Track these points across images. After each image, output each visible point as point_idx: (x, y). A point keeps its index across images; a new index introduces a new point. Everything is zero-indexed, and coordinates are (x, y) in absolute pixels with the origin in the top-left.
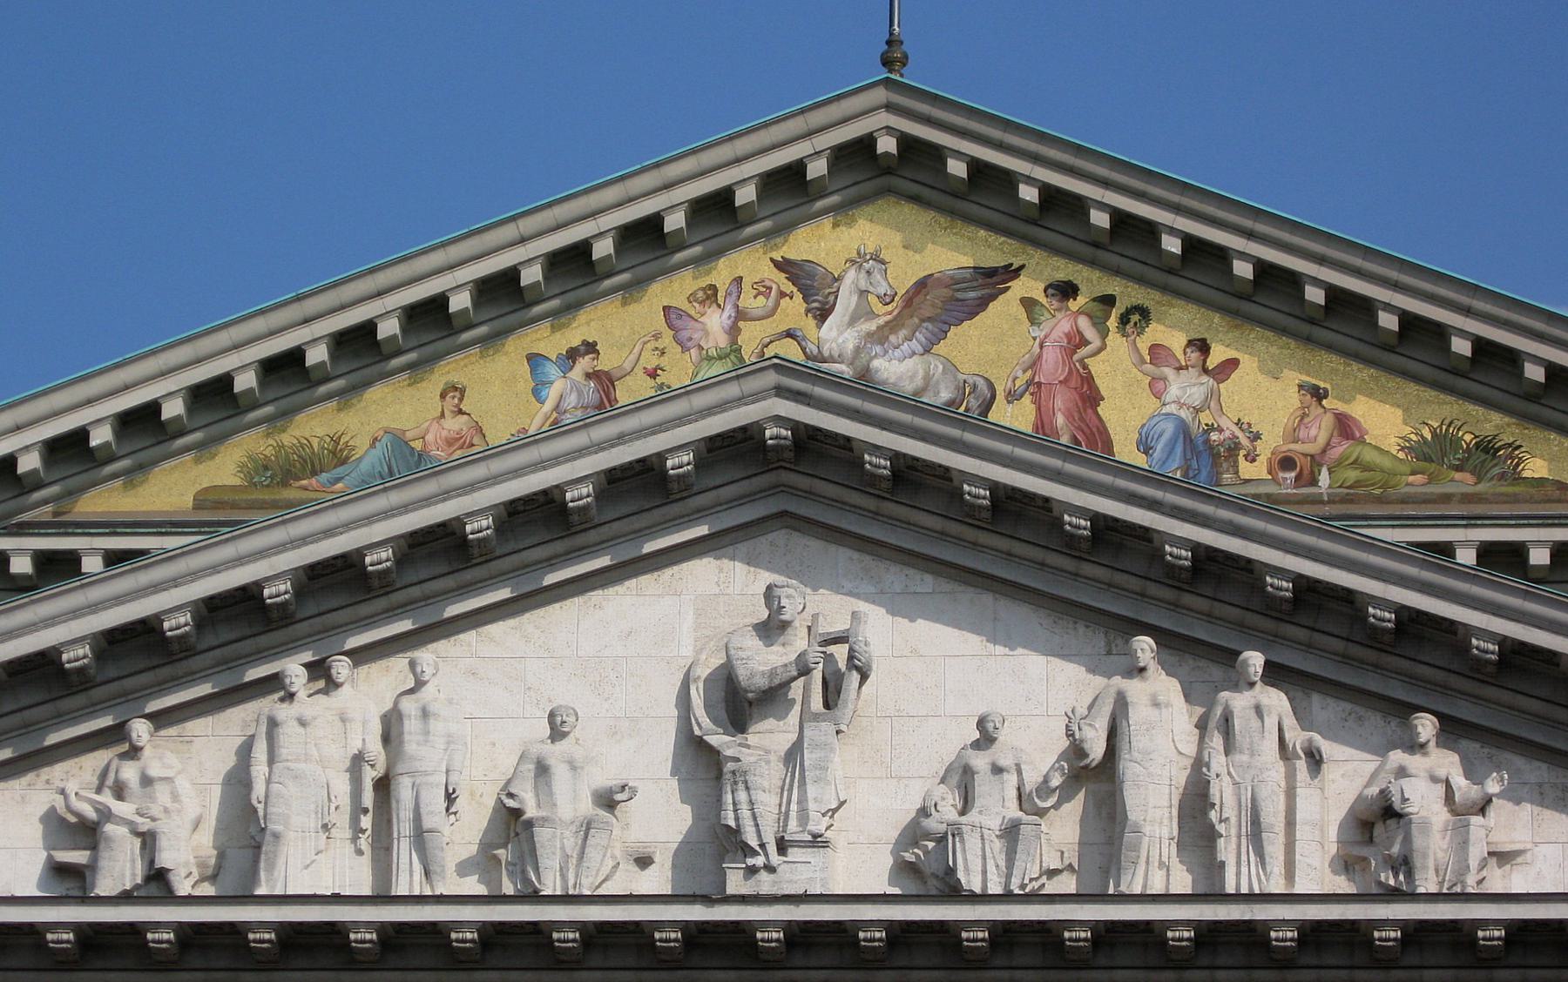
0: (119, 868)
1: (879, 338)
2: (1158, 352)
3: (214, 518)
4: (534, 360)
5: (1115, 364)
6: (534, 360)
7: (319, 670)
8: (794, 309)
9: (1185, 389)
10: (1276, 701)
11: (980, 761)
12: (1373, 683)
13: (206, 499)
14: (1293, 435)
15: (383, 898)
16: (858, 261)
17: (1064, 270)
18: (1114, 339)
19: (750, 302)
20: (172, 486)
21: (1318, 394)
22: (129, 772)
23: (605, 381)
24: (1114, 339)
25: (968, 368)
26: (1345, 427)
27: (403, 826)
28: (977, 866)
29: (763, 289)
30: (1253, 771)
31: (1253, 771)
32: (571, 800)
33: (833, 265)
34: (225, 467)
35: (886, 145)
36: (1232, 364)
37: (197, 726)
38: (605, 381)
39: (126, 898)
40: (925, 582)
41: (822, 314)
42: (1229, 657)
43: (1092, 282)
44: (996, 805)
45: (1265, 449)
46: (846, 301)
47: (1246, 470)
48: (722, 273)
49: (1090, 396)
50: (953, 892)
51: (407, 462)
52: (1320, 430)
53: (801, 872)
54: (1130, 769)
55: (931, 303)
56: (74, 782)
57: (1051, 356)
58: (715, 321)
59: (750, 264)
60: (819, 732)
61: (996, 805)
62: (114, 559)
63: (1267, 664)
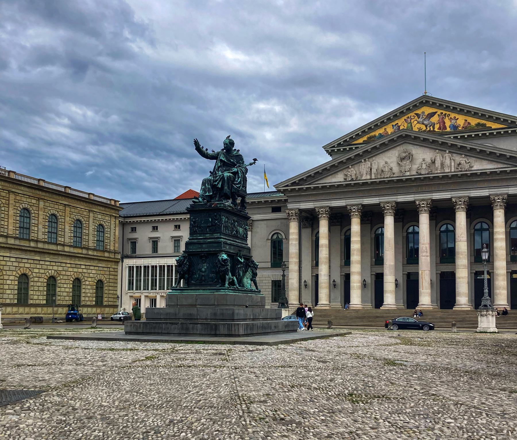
1: (424, 120)
3: (365, 142)
7: (365, 160)
9: (453, 121)
11: (423, 162)
12: (459, 152)
14: (464, 125)
15: (371, 179)
18: (447, 118)
19: (412, 117)
20: (361, 141)
21: (466, 120)
22: (350, 170)
24: (447, 118)
25: (433, 122)
26: (469, 123)
27: (373, 172)
28: (423, 172)
29: (413, 116)
30: (448, 162)
32: (387, 169)
34: (365, 138)
37: (355, 166)
38: (399, 126)
39: (350, 181)
42: (445, 151)
43: (444, 112)
45: (461, 126)
46: (421, 117)
48: (409, 115)
50: (421, 174)
51: (381, 136)
52: (467, 124)
53: (408, 174)
56: (345, 172)
58: (409, 120)
59: (412, 114)
60: (408, 161)
61: (424, 166)
62: (356, 148)
63: (449, 152)
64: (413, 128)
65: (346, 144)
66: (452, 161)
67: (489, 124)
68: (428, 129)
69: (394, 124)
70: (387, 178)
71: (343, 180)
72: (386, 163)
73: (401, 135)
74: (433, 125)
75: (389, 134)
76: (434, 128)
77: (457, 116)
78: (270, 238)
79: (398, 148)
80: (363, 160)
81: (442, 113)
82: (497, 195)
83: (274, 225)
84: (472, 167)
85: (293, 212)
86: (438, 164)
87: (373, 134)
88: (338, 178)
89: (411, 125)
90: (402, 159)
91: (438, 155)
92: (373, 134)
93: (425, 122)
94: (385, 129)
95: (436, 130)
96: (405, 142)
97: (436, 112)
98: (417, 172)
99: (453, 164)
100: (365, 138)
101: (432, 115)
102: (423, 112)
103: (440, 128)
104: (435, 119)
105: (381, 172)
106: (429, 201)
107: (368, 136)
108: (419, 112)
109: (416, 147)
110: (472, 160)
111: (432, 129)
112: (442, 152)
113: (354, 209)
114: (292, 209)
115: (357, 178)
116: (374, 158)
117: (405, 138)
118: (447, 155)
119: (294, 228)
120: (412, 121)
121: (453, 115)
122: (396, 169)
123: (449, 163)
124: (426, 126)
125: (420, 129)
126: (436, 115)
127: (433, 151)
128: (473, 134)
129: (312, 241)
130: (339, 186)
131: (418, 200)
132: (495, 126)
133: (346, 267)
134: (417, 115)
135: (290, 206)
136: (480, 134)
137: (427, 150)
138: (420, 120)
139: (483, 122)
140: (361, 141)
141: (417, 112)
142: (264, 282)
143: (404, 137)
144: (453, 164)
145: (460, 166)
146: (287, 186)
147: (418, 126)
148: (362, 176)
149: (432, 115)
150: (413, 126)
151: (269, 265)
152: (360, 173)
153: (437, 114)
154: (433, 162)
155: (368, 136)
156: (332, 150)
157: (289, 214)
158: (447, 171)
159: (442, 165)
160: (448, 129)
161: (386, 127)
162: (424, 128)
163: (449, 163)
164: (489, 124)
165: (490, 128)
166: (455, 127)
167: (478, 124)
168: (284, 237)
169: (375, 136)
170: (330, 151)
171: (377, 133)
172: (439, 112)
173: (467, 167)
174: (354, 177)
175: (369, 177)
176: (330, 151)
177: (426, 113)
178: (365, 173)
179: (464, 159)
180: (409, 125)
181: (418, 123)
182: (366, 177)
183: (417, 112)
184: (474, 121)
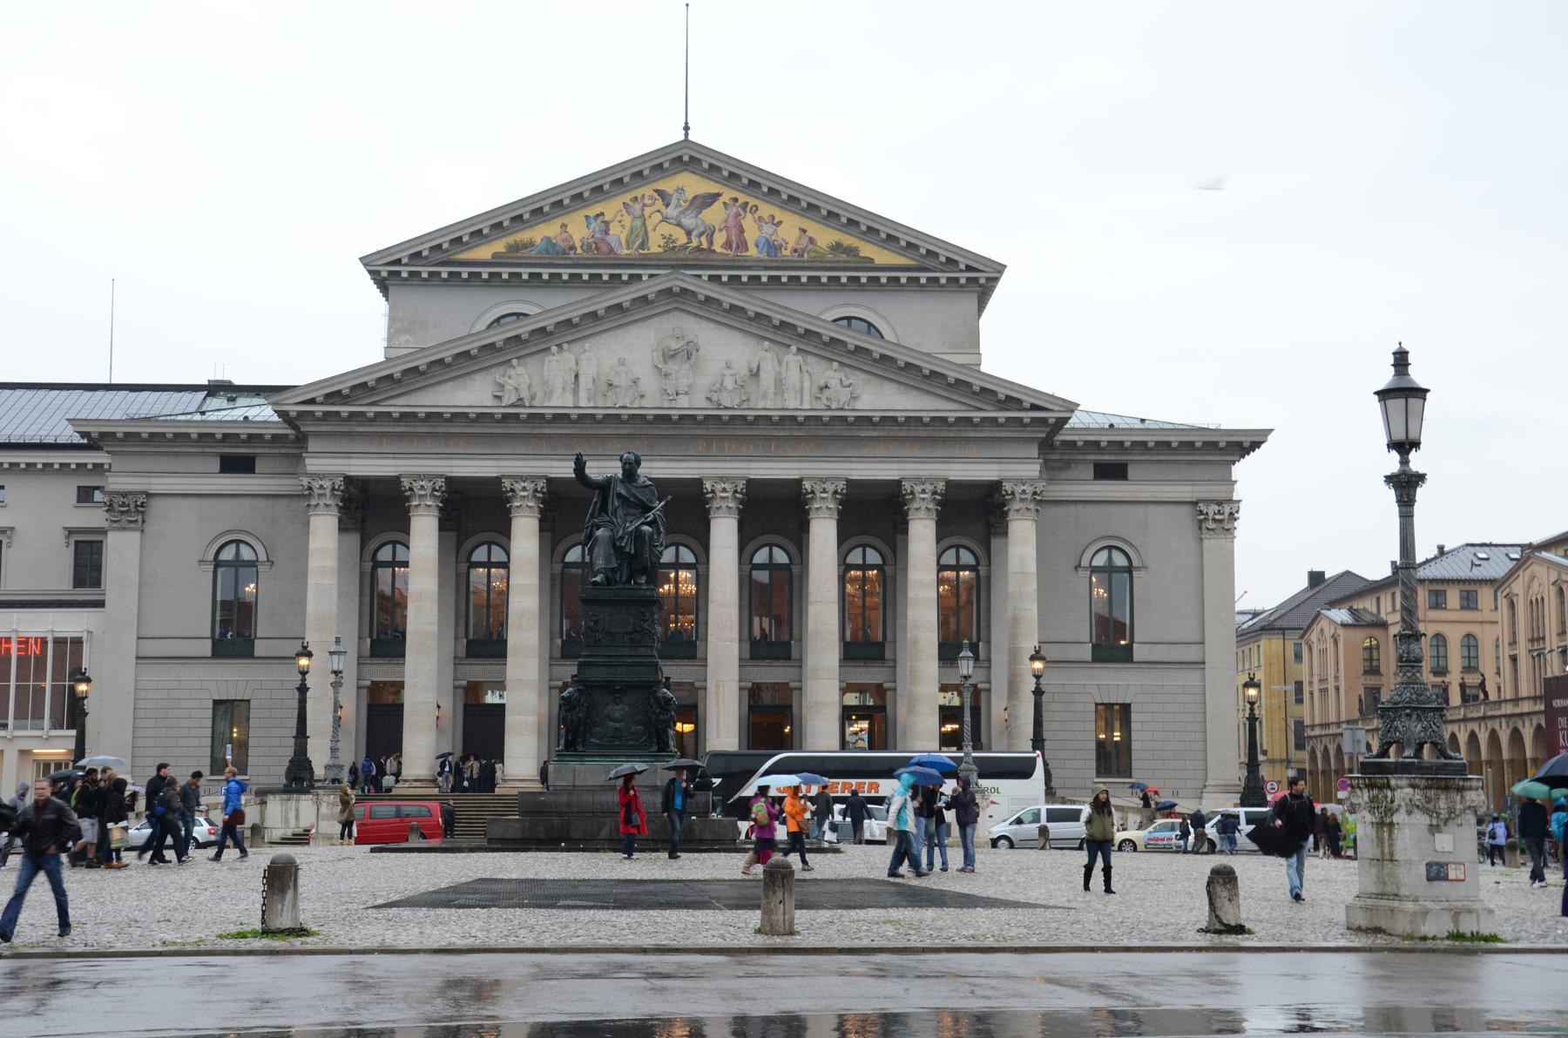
0: (510, 398)
1: (683, 213)
2: (760, 218)
4: (587, 217)
5: (748, 222)
6: (587, 217)
7: (559, 346)
8: (660, 202)
10: (799, 358)
11: (727, 372)
13: (495, 255)
16: (677, 190)
17: (735, 194)
19: (647, 201)
20: (484, 252)
21: (804, 231)
22: (512, 372)
23: (607, 223)
26: (811, 240)
29: (651, 197)
30: (793, 376)
31: (793, 376)
33: (670, 191)
34: (499, 246)
35: (686, 158)
36: (780, 222)
37: (528, 360)
38: (607, 223)
40: (712, 325)
41: (667, 205)
43: (742, 198)
44: (729, 383)
45: (790, 246)
46: (674, 202)
47: (786, 253)
48: (638, 193)
49: (742, 231)
52: (805, 241)
53: (683, 402)
54: (762, 374)
55: (697, 204)
57: (731, 219)
58: (638, 207)
59: (647, 191)
60: (687, 366)
61: (729, 383)
64: (651, 234)
65: (439, 257)
66: (806, 376)
67: (867, 250)
68: (695, 243)
69: (592, 211)
70: (624, 407)
71: (490, 401)
72: (622, 362)
73: (669, 290)
74: (710, 234)
75: (578, 244)
76: (711, 243)
77: (779, 215)
78: (211, 557)
79: (656, 322)
80: (554, 349)
81: (736, 200)
82: (918, 480)
83: (228, 517)
84: (854, 398)
85: (327, 484)
86: (767, 377)
87: (524, 236)
88: (473, 394)
89: (644, 224)
90: (670, 356)
91: (769, 355)
92: (524, 236)
93: (688, 221)
94: (564, 226)
95: (717, 247)
96: (676, 309)
97: (719, 195)
98: (709, 399)
99: (807, 385)
100: (499, 246)
101: (709, 200)
102: (681, 190)
103: (728, 245)
104: (714, 215)
105: (604, 388)
106: (741, 485)
107: (511, 239)
108: (668, 185)
109: (705, 324)
110: (857, 378)
111: (705, 246)
112: (777, 348)
113: (524, 489)
114: (322, 476)
115: (533, 398)
116: (587, 346)
117: (678, 299)
118: (792, 359)
119: (324, 532)
120: (647, 211)
121: (766, 210)
122: (650, 384)
123: (796, 384)
124: (689, 233)
125: (669, 239)
126: (718, 204)
127: (752, 341)
128: (824, 276)
129: (362, 574)
130: (481, 417)
131: (709, 478)
132: (882, 257)
133: (472, 661)
134: (660, 193)
135: (313, 464)
136: (844, 276)
137: (736, 337)
138: (671, 211)
139: (849, 240)
140: (484, 252)
141: (661, 186)
142: (184, 704)
143: (676, 295)
144: (807, 385)
145: (827, 393)
146: (312, 401)
147: (666, 229)
148: (549, 394)
149: (709, 200)
150: (650, 229)
151: (206, 648)
152: (544, 383)
153: (722, 199)
154: (755, 374)
155: (511, 239)
156: (391, 273)
157: (310, 488)
158: (792, 403)
159: (779, 384)
160: (753, 252)
161: (565, 219)
162: (683, 239)
163: (797, 380)
164: (867, 250)
165: (868, 264)
166: (773, 247)
167: (837, 247)
168: (263, 557)
169: (531, 244)
170: (384, 274)
171: (539, 234)
172: (727, 194)
173: (844, 396)
174: (525, 394)
175: (568, 401)
176: (384, 274)
177: (689, 195)
178: (559, 386)
179: (840, 375)
180: (638, 223)
181: (665, 219)
182: (560, 400)
183: (661, 186)
184: (825, 237)
